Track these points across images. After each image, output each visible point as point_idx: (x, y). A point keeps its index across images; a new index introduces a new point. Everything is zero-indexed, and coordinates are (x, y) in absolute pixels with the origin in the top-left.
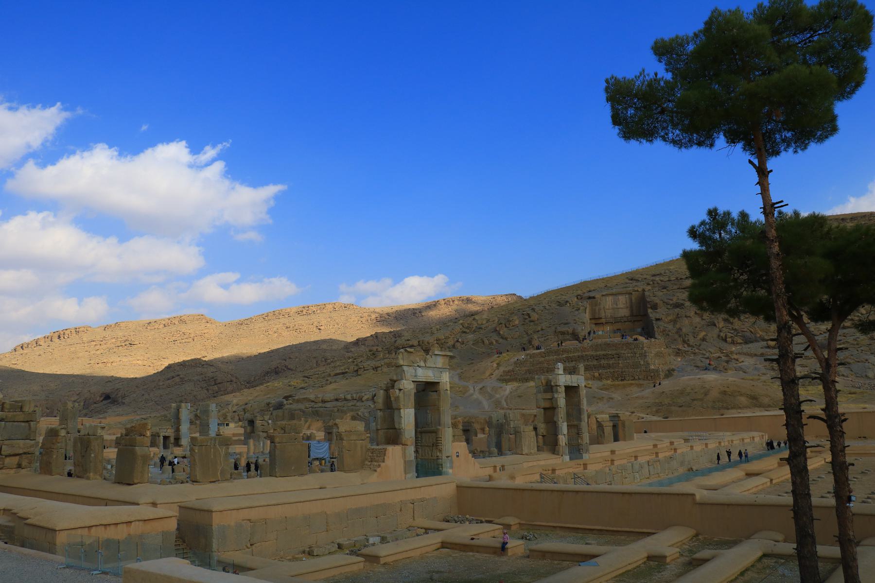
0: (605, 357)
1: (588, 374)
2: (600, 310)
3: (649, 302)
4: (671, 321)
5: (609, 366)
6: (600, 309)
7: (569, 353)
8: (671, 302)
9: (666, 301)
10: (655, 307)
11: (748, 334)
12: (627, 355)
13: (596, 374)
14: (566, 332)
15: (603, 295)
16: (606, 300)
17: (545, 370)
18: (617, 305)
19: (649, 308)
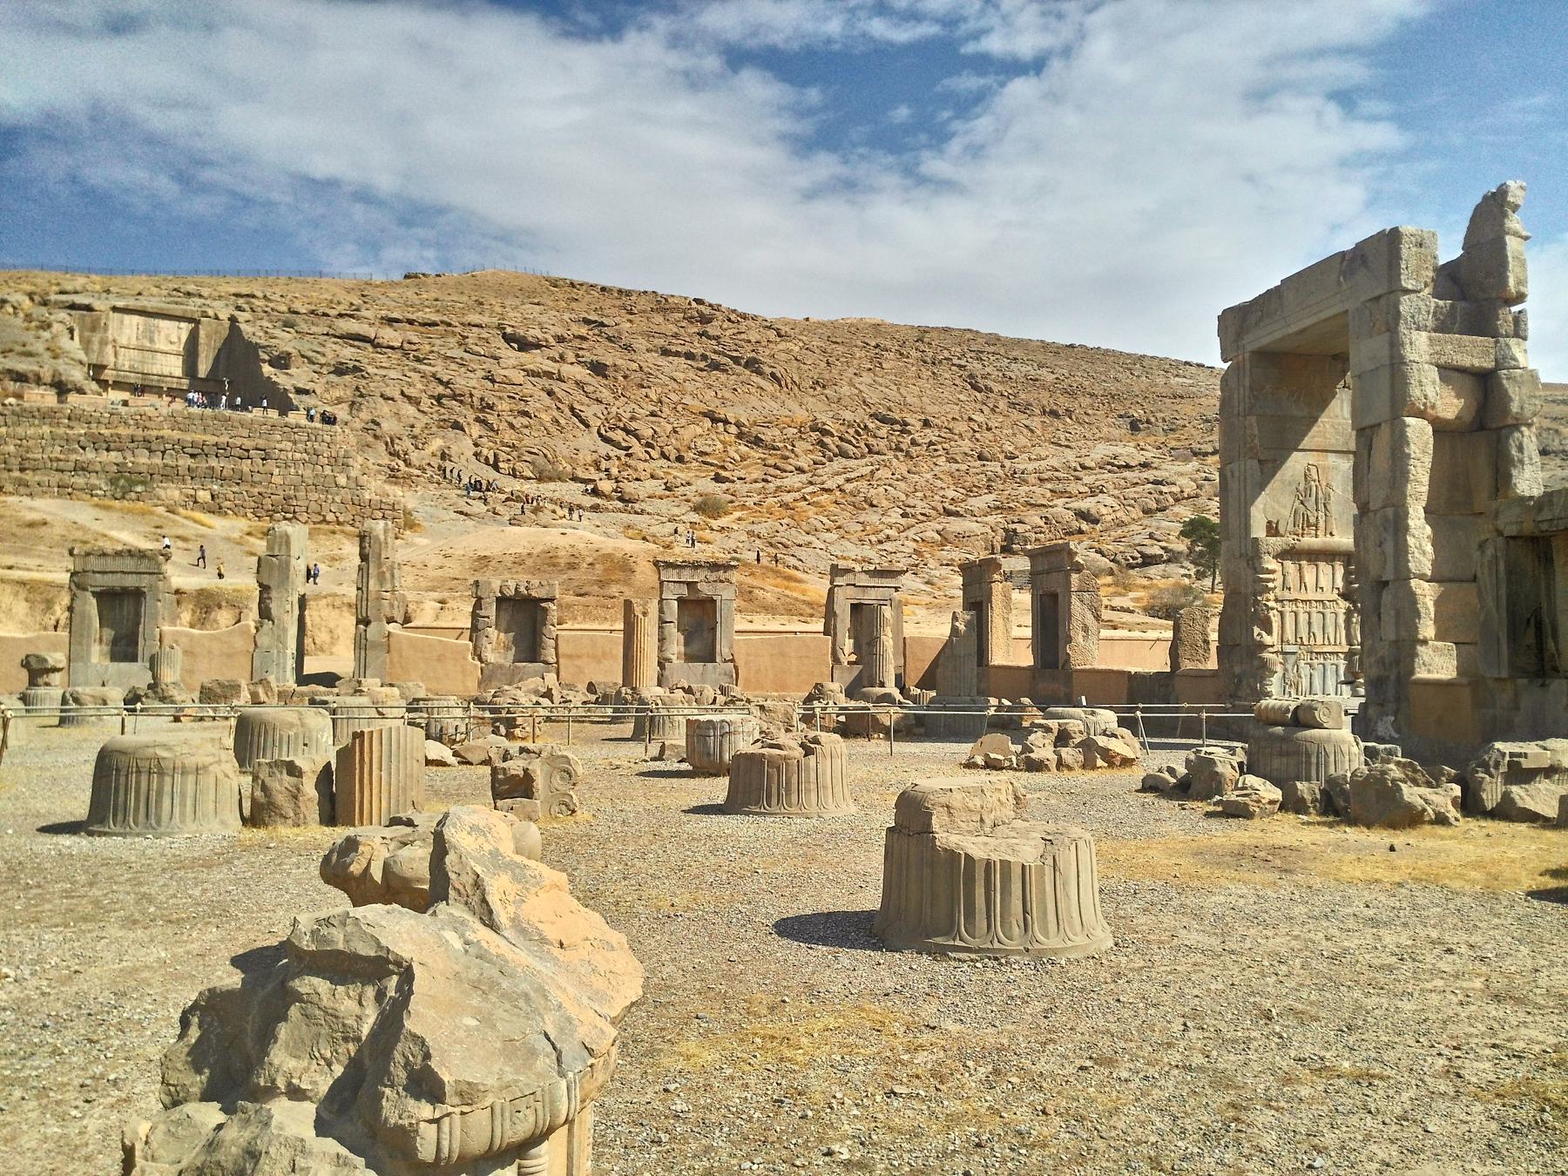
0: (221, 450)
1: (177, 493)
2: (103, 343)
3: (264, 347)
4: (339, 401)
5: (241, 480)
6: (106, 344)
7: (94, 425)
8: (323, 360)
9: (311, 354)
10: (282, 362)
11: (541, 460)
12: (290, 455)
13: (204, 496)
14: (30, 375)
15: (115, 309)
16: (122, 322)
17: (15, 463)
18: (152, 340)
19: (264, 361)
